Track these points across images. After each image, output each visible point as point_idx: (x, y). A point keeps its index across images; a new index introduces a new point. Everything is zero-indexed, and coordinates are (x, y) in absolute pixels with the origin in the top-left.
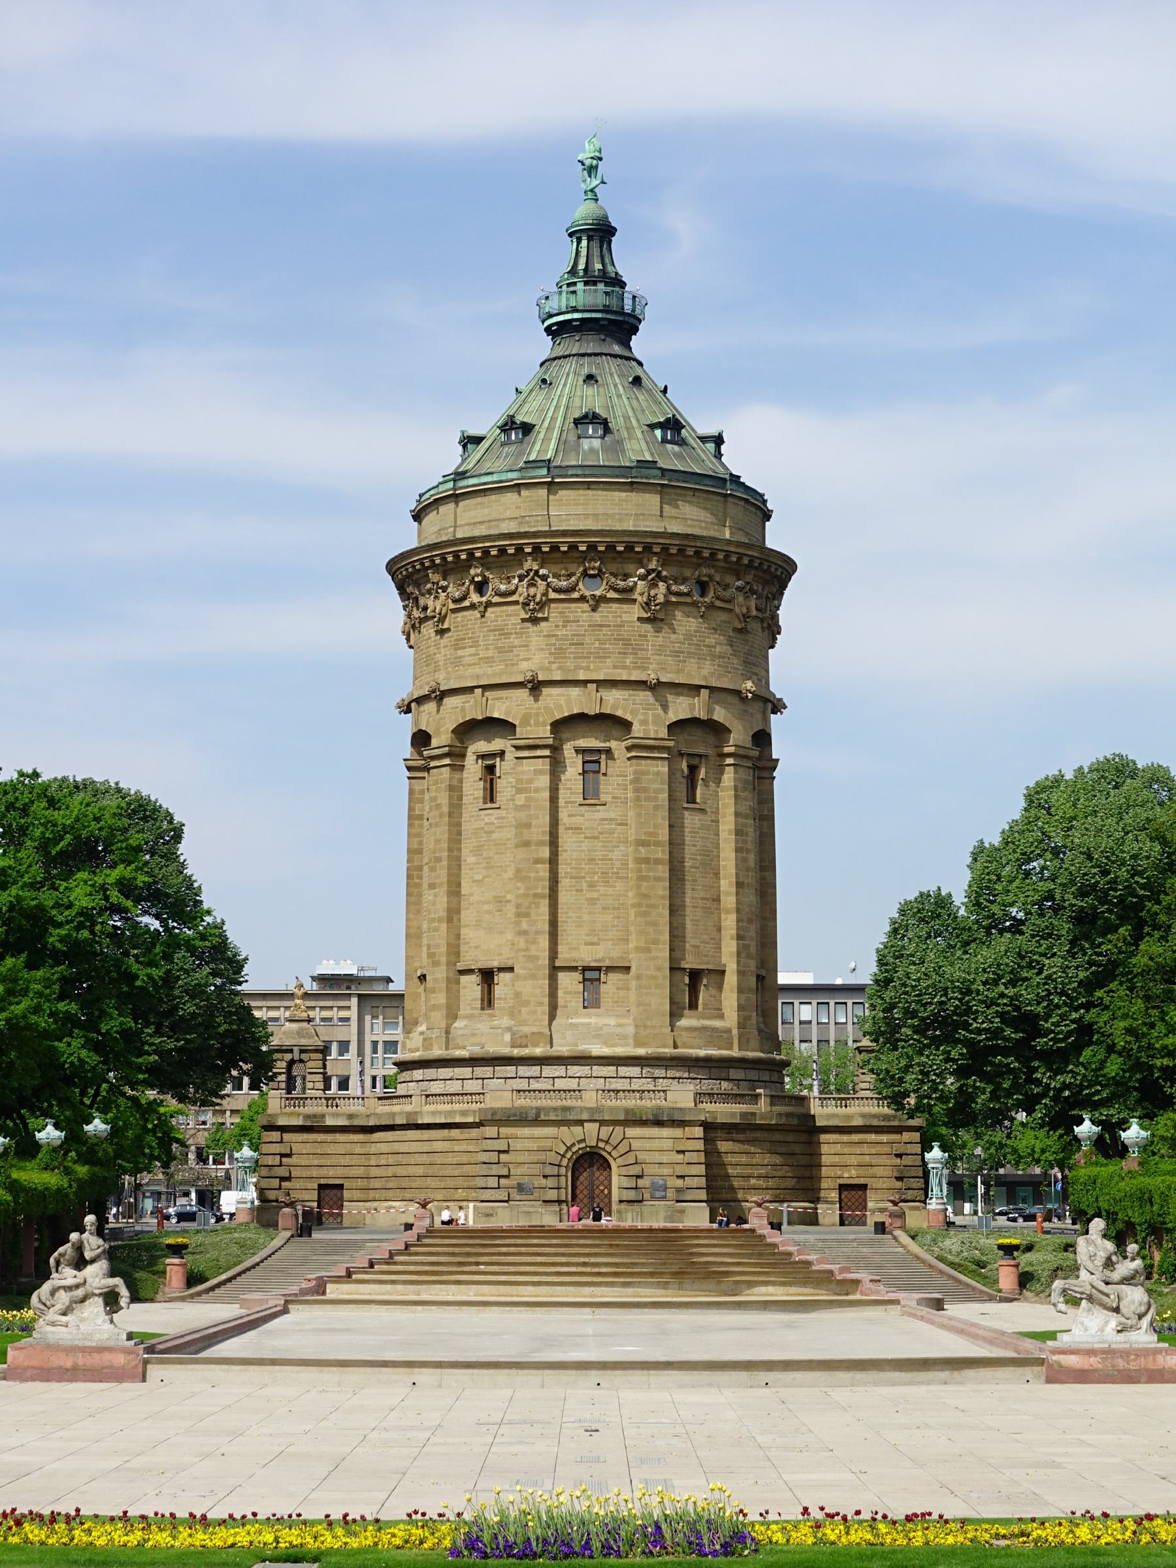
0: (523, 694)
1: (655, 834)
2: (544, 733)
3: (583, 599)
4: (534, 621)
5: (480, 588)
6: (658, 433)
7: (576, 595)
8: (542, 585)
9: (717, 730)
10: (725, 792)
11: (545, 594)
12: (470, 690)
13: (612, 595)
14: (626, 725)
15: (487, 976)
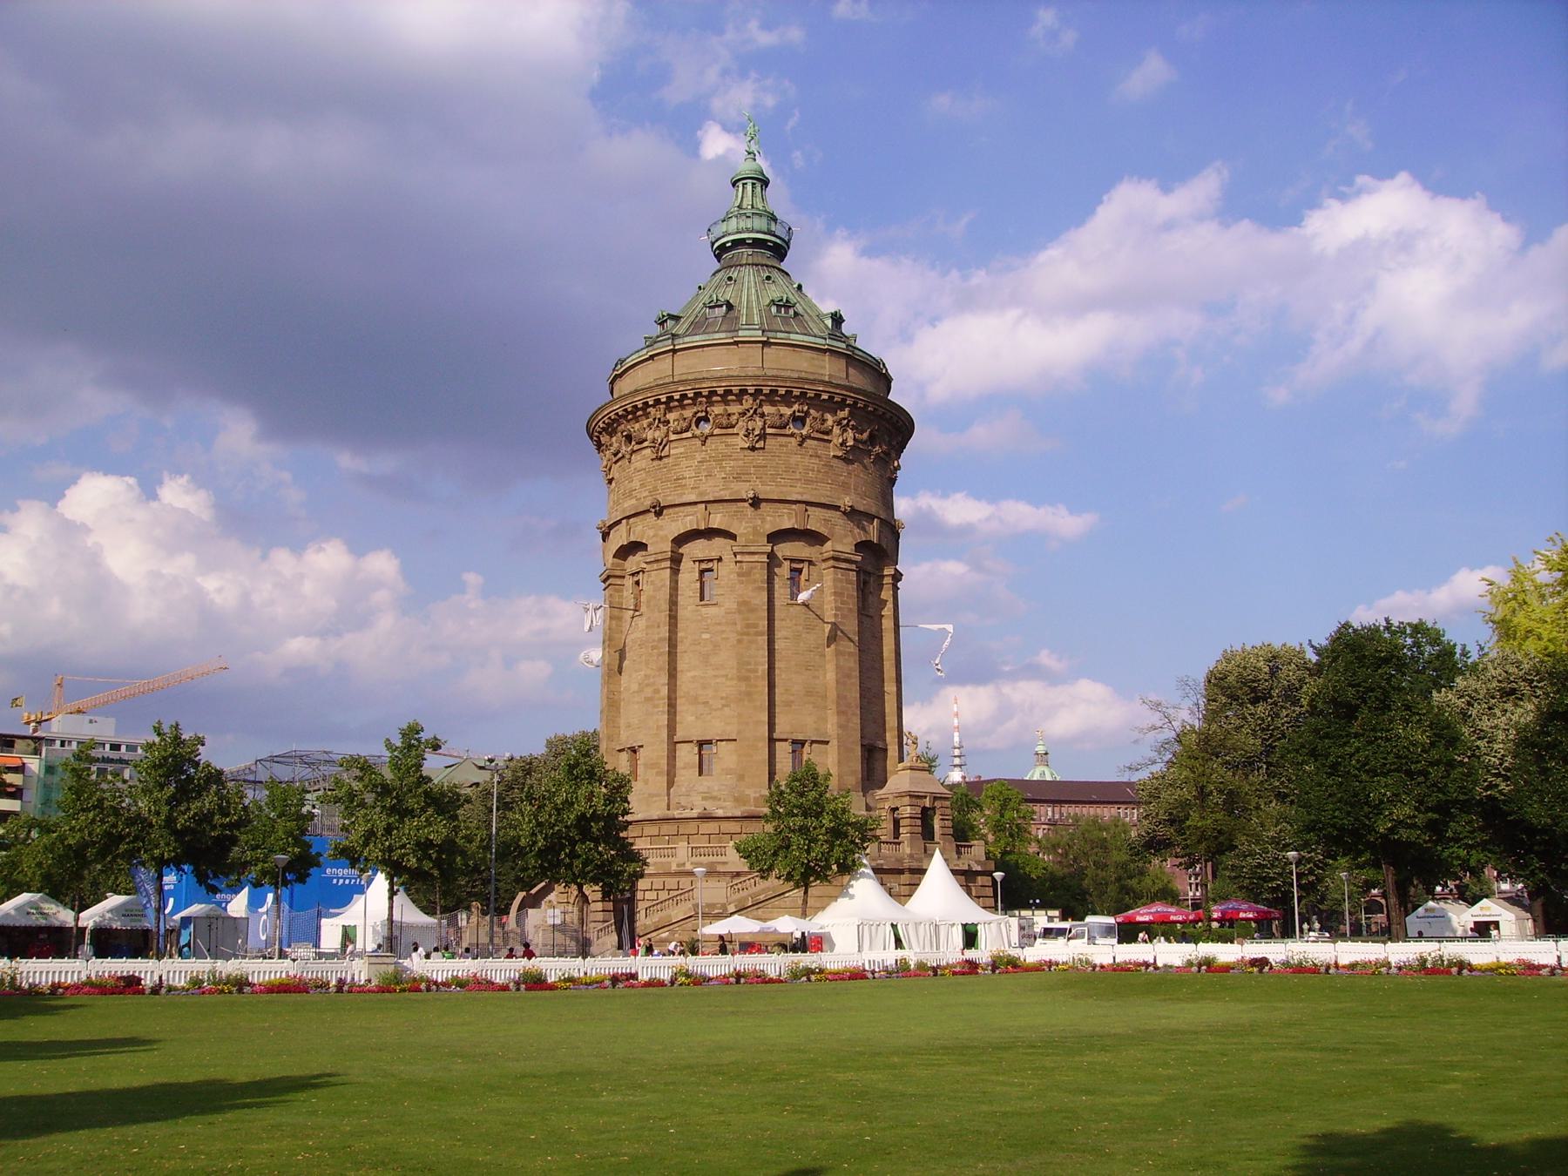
0: (651, 517)
1: (755, 626)
2: (667, 547)
3: (694, 436)
4: (661, 458)
5: (629, 438)
6: (774, 309)
7: (689, 434)
8: (664, 428)
9: (815, 538)
10: (825, 589)
11: (667, 435)
12: (618, 522)
13: (717, 431)
14: (733, 537)
15: (634, 750)
